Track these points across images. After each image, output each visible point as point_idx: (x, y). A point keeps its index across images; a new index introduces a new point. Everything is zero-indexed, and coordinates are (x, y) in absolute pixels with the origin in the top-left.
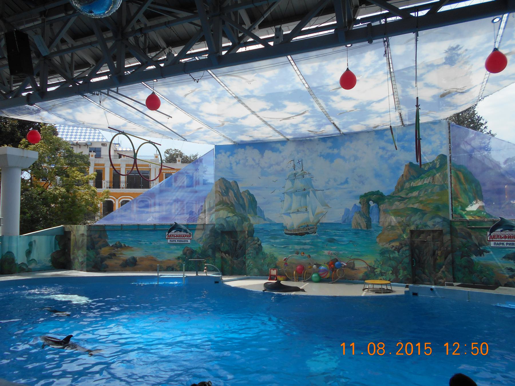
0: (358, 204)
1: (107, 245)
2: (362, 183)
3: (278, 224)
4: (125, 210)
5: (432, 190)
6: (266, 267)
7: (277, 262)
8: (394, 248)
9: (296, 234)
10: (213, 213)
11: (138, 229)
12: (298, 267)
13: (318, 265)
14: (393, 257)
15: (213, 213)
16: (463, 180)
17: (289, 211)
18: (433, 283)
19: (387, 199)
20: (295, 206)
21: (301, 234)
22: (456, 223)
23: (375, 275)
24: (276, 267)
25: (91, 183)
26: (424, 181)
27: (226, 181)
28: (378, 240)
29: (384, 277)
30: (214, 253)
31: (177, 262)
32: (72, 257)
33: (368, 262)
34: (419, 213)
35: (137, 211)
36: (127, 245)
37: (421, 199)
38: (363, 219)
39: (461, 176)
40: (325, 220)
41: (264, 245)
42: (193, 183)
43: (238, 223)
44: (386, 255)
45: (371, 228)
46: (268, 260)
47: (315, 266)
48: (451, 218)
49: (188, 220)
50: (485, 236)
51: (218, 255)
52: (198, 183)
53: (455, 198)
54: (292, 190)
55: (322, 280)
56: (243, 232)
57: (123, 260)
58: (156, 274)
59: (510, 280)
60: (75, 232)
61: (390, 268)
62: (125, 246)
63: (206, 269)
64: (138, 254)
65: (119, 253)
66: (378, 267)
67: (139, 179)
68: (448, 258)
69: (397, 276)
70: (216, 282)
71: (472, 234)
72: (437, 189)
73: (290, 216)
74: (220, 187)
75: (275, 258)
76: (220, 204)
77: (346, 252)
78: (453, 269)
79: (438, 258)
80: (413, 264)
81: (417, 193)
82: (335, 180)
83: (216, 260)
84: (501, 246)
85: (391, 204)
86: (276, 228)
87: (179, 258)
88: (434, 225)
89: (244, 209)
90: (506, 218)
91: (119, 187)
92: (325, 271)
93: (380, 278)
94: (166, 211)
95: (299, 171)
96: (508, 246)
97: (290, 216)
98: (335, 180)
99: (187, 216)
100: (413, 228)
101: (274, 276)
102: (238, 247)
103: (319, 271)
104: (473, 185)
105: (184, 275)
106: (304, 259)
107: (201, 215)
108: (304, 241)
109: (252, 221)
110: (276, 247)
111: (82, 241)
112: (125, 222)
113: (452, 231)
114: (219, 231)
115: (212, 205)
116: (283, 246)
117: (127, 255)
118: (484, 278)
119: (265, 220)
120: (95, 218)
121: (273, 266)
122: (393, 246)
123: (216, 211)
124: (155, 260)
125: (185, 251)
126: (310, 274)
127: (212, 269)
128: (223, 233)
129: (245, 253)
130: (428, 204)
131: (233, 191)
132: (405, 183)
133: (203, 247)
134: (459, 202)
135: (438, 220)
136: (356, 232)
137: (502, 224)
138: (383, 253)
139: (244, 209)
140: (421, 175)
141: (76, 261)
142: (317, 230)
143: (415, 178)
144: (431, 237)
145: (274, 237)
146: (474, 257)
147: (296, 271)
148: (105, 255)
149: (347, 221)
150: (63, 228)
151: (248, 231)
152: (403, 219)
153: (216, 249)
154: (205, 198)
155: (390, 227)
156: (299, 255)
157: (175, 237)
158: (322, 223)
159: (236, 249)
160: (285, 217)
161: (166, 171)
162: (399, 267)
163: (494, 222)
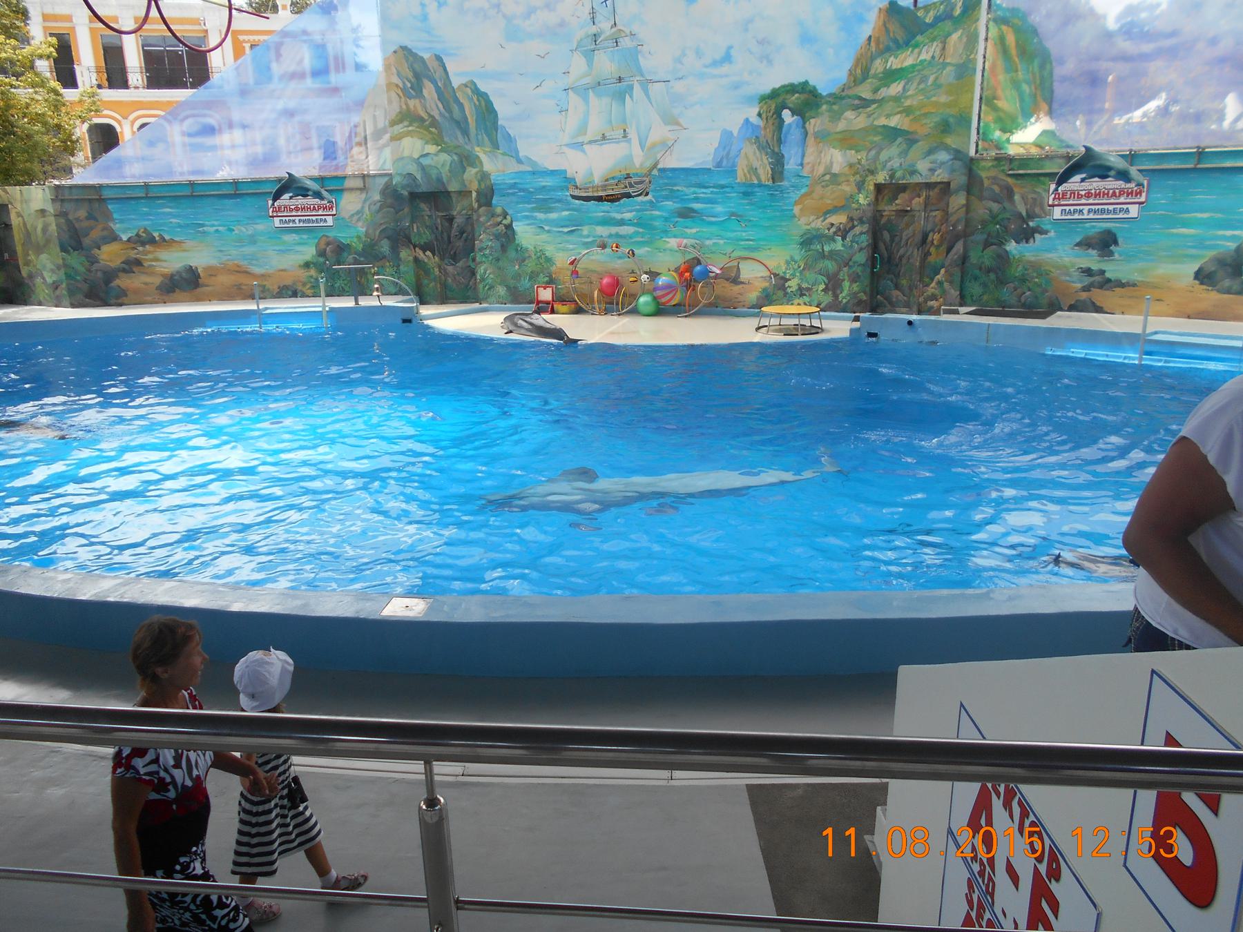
0: (755, 120)
1: (114, 238)
2: (767, 59)
3: (553, 173)
4: (151, 144)
6: (525, 283)
7: (553, 269)
8: (833, 230)
9: (600, 199)
10: (384, 146)
11: (194, 194)
12: (605, 281)
13: (653, 275)
14: (831, 252)
15: (384, 146)
16: (1013, 52)
17: (580, 139)
18: (915, 309)
19: (827, 102)
20: (596, 126)
21: (612, 199)
22: (983, 164)
23: (786, 294)
24: (551, 282)
25: (44, 67)
27: (415, 55)
28: (796, 210)
29: (806, 299)
30: (395, 249)
31: (303, 274)
32: (24, 272)
33: (772, 264)
34: (900, 140)
35: (184, 145)
36: (167, 237)
37: (908, 103)
38: (764, 158)
39: (1011, 39)
40: (671, 162)
41: (518, 227)
42: (326, 66)
44: (813, 247)
46: (530, 265)
47: (645, 277)
48: (972, 153)
49: (321, 167)
50: (1044, 194)
51: (405, 254)
52: (340, 65)
53: (988, 100)
55: (661, 310)
56: (465, 193)
57: (163, 275)
58: (253, 307)
59: (1084, 296)
61: (820, 277)
63: (377, 290)
64: (200, 257)
65: (150, 256)
66: (794, 275)
67: (179, 65)
68: (954, 250)
69: (836, 296)
70: (406, 321)
71: (1016, 190)
72: (948, 75)
73: (583, 151)
74: (399, 74)
75: (548, 260)
76: (401, 121)
77: (722, 242)
78: (963, 272)
79: (932, 250)
80: (874, 266)
81: (900, 88)
82: (699, 54)
83: (401, 267)
84: (1076, 216)
85: (836, 116)
86: (548, 182)
87: (307, 265)
88: (932, 170)
89: (466, 133)
90: (1097, 148)
91: (124, 84)
92: (670, 288)
93: (796, 301)
94: (264, 143)
95: (605, 25)
96: (1091, 216)
97: (583, 151)
98: (699, 54)
99: (317, 156)
100: (881, 178)
101: (548, 303)
102: (454, 232)
103: (655, 289)
104: (1036, 63)
105: (324, 306)
106: (619, 261)
107: (356, 150)
108: (618, 216)
109: (488, 164)
110: (549, 231)
111: (45, 230)
112: (152, 180)
113: (972, 184)
114: (406, 193)
115: (381, 125)
116: (566, 230)
117: (171, 261)
119: (520, 161)
120: (71, 171)
122: (832, 225)
123: (393, 139)
124: (247, 272)
126: (634, 297)
127: (393, 290)
128: (415, 197)
129: (473, 250)
130: (925, 115)
131: (434, 82)
132: (872, 59)
133: (367, 235)
134: (995, 109)
135: (943, 156)
137: (1086, 164)
138: (807, 241)
139: (466, 133)
140: (914, 36)
141: (39, 280)
142: (652, 187)
143: (899, 47)
144: (921, 200)
145: (545, 206)
146: (1012, 247)
148: (113, 265)
149: (725, 163)
152: (862, 156)
153: (400, 239)
154: (360, 104)
156: (608, 250)
157: (291, 210)
158: (663, 170)
159: (449, 237)
160: (571, 153)
161: (251, 38)
163: (1068, 158)
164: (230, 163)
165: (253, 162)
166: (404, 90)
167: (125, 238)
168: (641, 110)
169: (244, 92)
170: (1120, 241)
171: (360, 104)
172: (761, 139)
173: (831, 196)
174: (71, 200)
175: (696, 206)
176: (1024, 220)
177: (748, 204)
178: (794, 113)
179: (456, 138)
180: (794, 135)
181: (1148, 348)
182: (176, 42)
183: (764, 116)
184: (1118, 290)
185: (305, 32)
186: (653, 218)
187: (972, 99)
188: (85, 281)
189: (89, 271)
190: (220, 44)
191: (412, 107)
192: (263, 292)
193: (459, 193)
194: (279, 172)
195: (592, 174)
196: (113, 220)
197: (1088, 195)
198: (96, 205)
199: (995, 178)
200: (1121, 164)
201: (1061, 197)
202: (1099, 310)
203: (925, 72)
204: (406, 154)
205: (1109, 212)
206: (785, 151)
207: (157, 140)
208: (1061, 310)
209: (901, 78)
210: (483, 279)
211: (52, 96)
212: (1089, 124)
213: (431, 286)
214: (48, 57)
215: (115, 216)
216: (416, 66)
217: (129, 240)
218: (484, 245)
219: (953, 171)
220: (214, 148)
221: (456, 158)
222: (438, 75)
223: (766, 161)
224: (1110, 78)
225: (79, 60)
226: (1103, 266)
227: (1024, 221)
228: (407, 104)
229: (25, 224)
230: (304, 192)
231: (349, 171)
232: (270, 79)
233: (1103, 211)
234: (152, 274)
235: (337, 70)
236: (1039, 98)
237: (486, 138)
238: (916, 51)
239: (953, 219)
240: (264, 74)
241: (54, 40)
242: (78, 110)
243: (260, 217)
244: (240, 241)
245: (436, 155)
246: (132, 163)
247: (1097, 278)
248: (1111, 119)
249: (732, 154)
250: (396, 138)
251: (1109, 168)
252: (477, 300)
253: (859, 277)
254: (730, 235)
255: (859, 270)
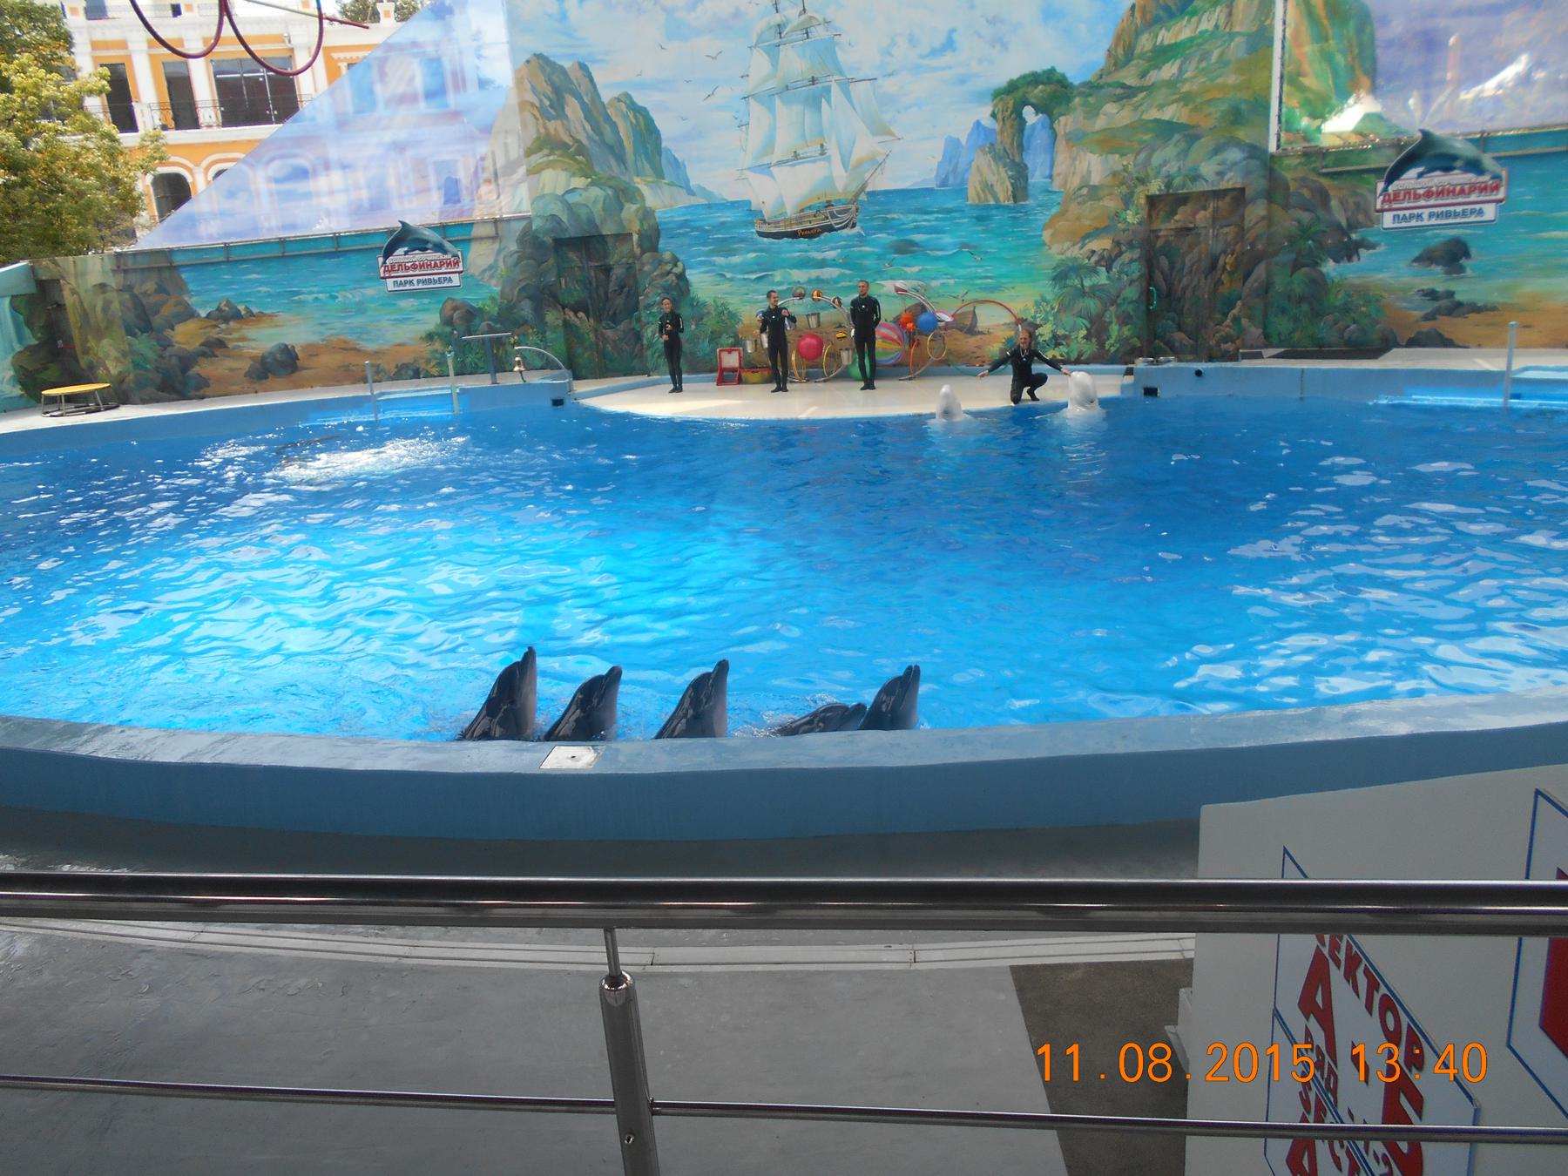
0: (987, 122)
1: (190, 314)
2: (1001, 43)
3: (734, 205)
4: (231, 195)
5: (1222, 53)
6: (705, 346)
7: (739, 326)
8: (1095, 258)
9: (794, 235)
10: (520, 182)
11: (288, 254)
14: (1093, 287)
15: (520, 182)
17: (766, 160)
19: (1081, 94)
20: (785, 141)
21: (810, 234)
22: (1287, 162)
25: (95, 104)
26: (1199, 22)
30: (538, 311)
31: (426, 349)
32: (84, 362)
34: (1177, 137)
35: (271, 194)
36: (255, 310)
37: (1186, 88)
40: (882, 183)
41: (693, 276)
42: (441, 86)
43: (604, 209)
45: (1026, 197)
46: (710, 323)
48: (1272, 148)
49: (441, 213)
50: (1370, 197)
52: (460, 82)
53: (1291, 78)
54: (771, 84)
56: (624, 237)
57: (254, 358)
59: (1427, 326)
60: (72, 280)
61: (1080, 320)
62: (251, 314)
64: (296, 333)
65: (235, 335)
66: (1046, 320)
69: (1101, 344)
70: (558, 402)
71: (1332, 193)
72: (1237, 48)
73: (771, 175)
74: (533, 89)
76: (540, 149)
77: (951, 282)
79: (1225, 278)
81: (1175, 69)
83: (549, 335)
84: (1413, 223)
85: (1093, 112)
86: (728, 217)
87: (430, 337)
88: (1221, 174)
90: (1438, 132)
95: (791, 13)
96: (1433, 221)
97: (771, 175)
98: (913, 41)
99: (436, 198)
100: (1155, 187)
101: (734, 370)
102: (612, 287)
107: (484, 189)
108: (818, 256)
110: (731, 280)
111: (106, 309)
112: (232, 240)
113: (1275, 189)
114: (548, 240)
116: (753, 276)
117: (261, 340)
118: (1353, 327)
119: (691, 193)
121: (727, 340)
122: (1093, 252)
125: (448, 312)
128: (560, 243)
129: (636, 308)
131: (579, 98)
132: (1138, 34)
133: (502, 292)
134: (1302, 89)
135: (1234, 155)
136: (982, 217)
137: (1425, 153)
138: (1061, 276)
139: (621, 159)
142: (860, 216)
145: (724, 248)
146: (1330, 267)
147: (799, 352)
148: (189, 348)
149: (951, 180)
150: (33, 269)
151: (639, 233)
152: (1129, 160)
153: (544, 297)
154: (487, 130)
155: (1085, 191)
156: (807, 299)
157: (407, 269)
158: (873, 194)
159: (606, 293)
160: (756, 179)
162: (1107, 315)
163: (1397, 146)
164: (328, 213)
165: (357, 211)
166: (541, 109)
167: (203, 314)
168: (839, 115)
169: (342, 124)
170: (1473, 251)
171: (487, 130)
172: (998, 147)
173: (1088, 214)
174: (135, 270)
175: (918, 237)
176: (1344, 232)
177: (984, 232)
178: (1038, 110)
179: (610, 168)
180: (1040, 139)
181: (1517, 390)
182: (255, 65)
183: (999, 116)
184: (1473, 316)
185: (415, 44)
186: (865, 256)
187: (1270, 78)
188: (157, 369)
189: (161, 357)
190: (310, 65)
191: (552, 131)
192: (377, 373)
193: (617, 236)
194: (389, 221)
195: (783, 204)
196: (188, 292)
197: (1429, 194)
198: (167, 274)
199: (1303, 179)
200: (1468, 151)
201: (1391, 199)
202: (1447, 343)
203: (1206, 47)
204: (547, 191)
205: (1456, 215)
206: (1029, 161)
207: (239, 190)
208: (1398, 345)
209: (1175, 57)
210: (651, 345)
211: (106, 141)
212: (1426, 100)
213: (585, 357)
214: (100, 92)
215: (191, 287)
216: (555, 78)
217: (209, 316)
218: (650, 301)
219: (1247, 173)
220: (307, 195)
221: (610, 192)
222: (584, 88)
223: (1003, 175)
224: (1452, 40)
225: (138, 97)
226: (1452, 286)
227: (1344, 232)
228: (545, 128)
229: (81, 303)
230: (421, 245)
231: (477, 216)
232: (373, 104)
233: (1448, 215)
234: (240, 357)
235: (457, 89)
236: (1359, 72)
237: (647, 166)
238: (1194, 19)
239: (1250, 236)
240: (365, 99)
241: (106, 71)
242: (139, 158)
243: (369, 279)
244: (344, 310)
245: (585, 189)
246: (209, 220)
247: (1444, 303)
248: (1455, 95)
249: (961, 168)
250: (534, 171)
251: (1454, 158)
252: (646, 372)
253: (1130, 317)
254: (963, 272)
255: (1130, 308)
